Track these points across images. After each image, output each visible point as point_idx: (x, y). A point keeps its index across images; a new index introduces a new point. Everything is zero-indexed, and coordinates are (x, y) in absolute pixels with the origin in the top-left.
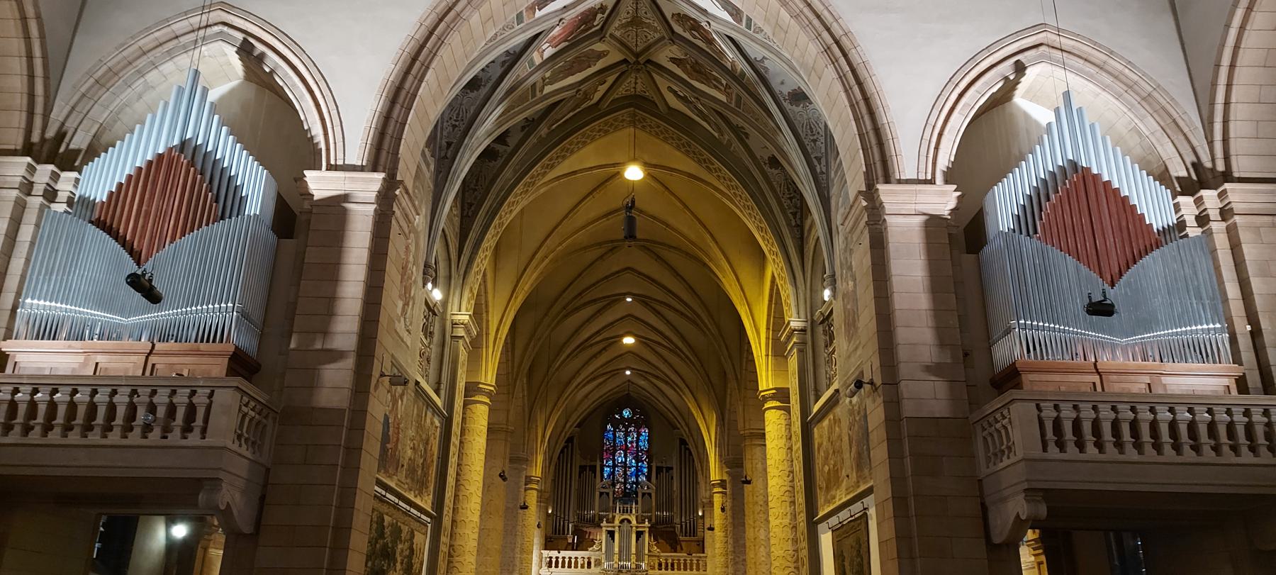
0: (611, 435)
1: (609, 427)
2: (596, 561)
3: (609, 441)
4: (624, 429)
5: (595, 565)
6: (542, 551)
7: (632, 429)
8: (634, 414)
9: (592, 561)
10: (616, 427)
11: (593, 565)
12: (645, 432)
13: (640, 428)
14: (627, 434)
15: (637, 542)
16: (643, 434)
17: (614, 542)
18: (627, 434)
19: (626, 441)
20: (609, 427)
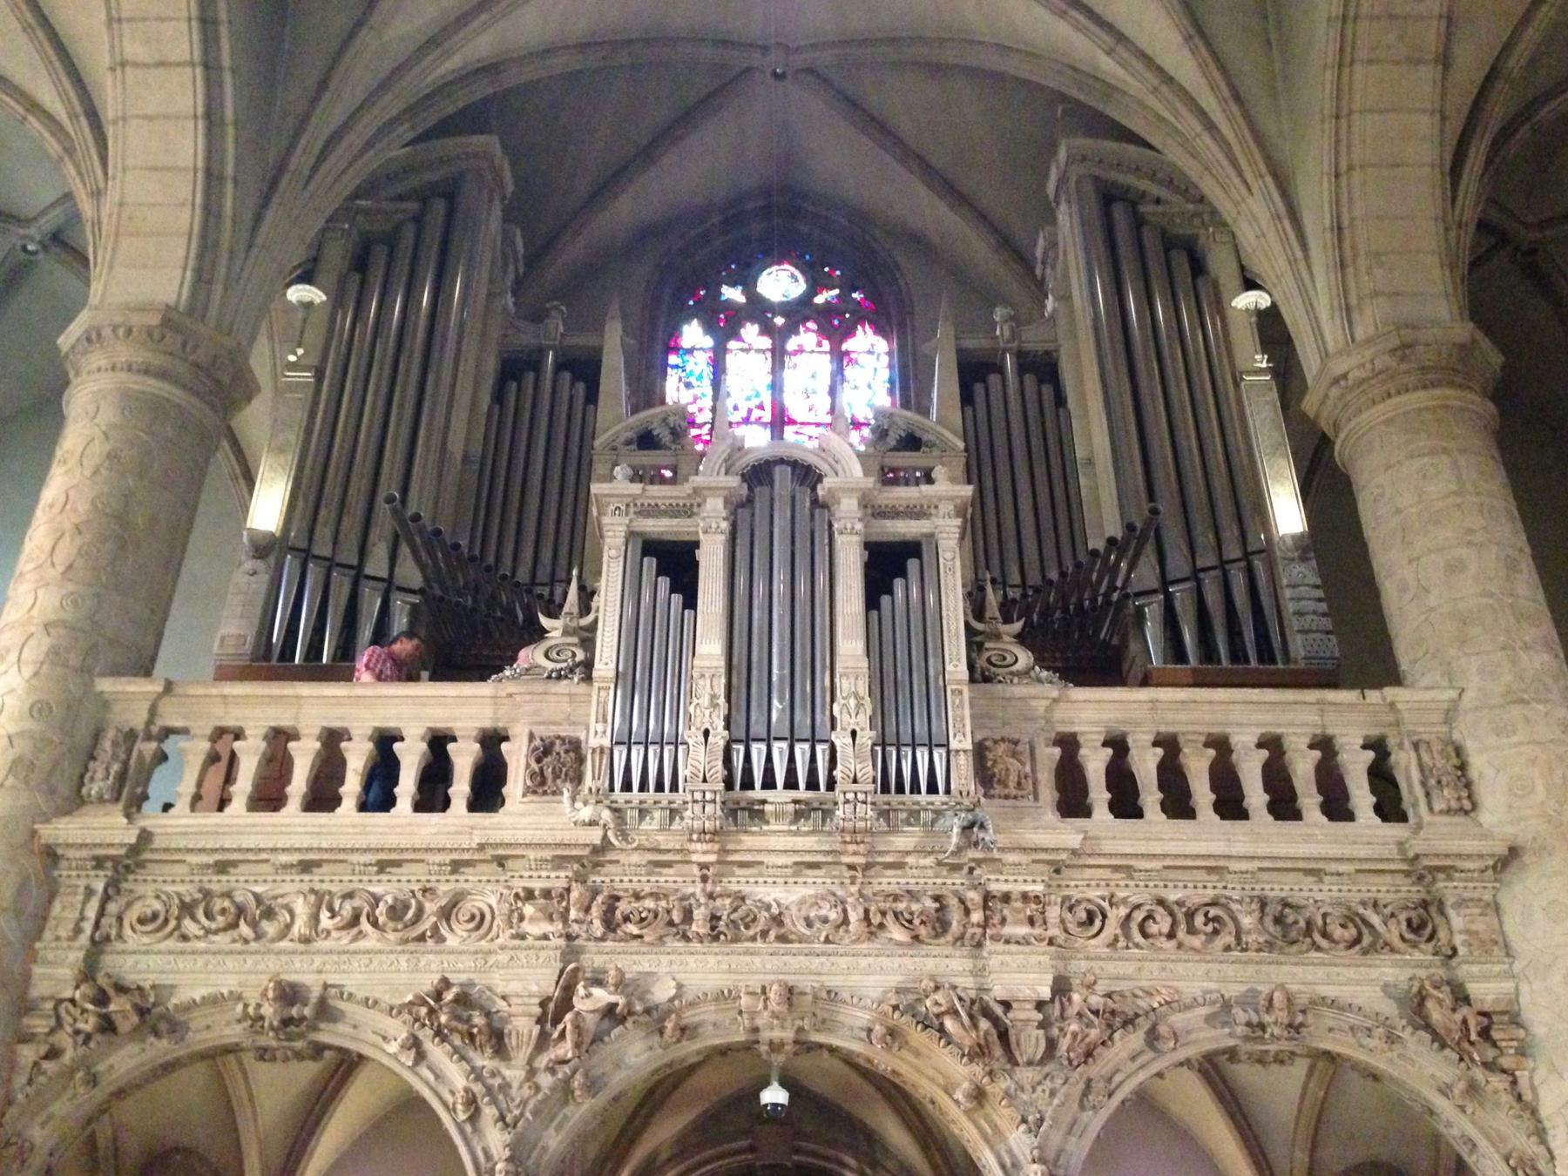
0: (700, 364)
1: (693, 334)
2: (543, 751)
3: (688, 385)
4: (766, 342)
5: (539, 784)
6: (106, 685)
7: (807, 338)
8: (815, 288)
9: (516, 755)
10: (724, 325)
11: (514, 787)
12: (870, 352)
13: (850, 333)
14: (778, 356)
15: (872, 603)
16: (863, 359)
17: (691, 602)
18: (778, 356)
19: (776, 387)
20: (693, 334)
